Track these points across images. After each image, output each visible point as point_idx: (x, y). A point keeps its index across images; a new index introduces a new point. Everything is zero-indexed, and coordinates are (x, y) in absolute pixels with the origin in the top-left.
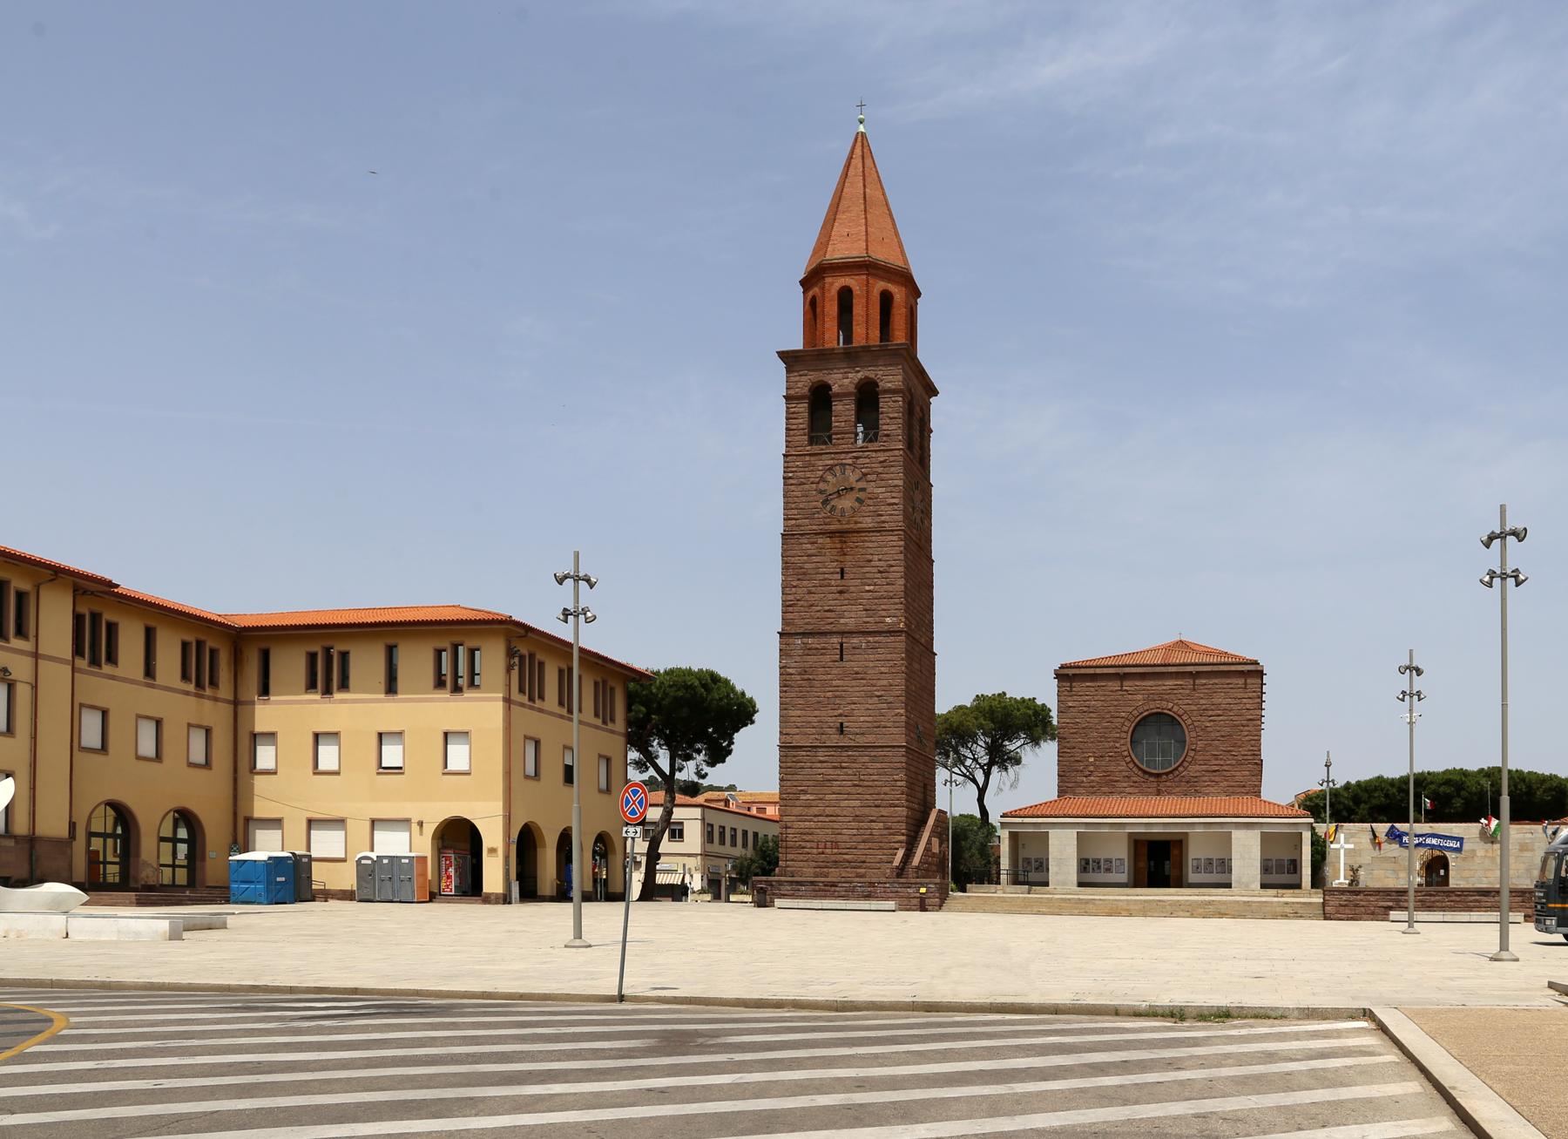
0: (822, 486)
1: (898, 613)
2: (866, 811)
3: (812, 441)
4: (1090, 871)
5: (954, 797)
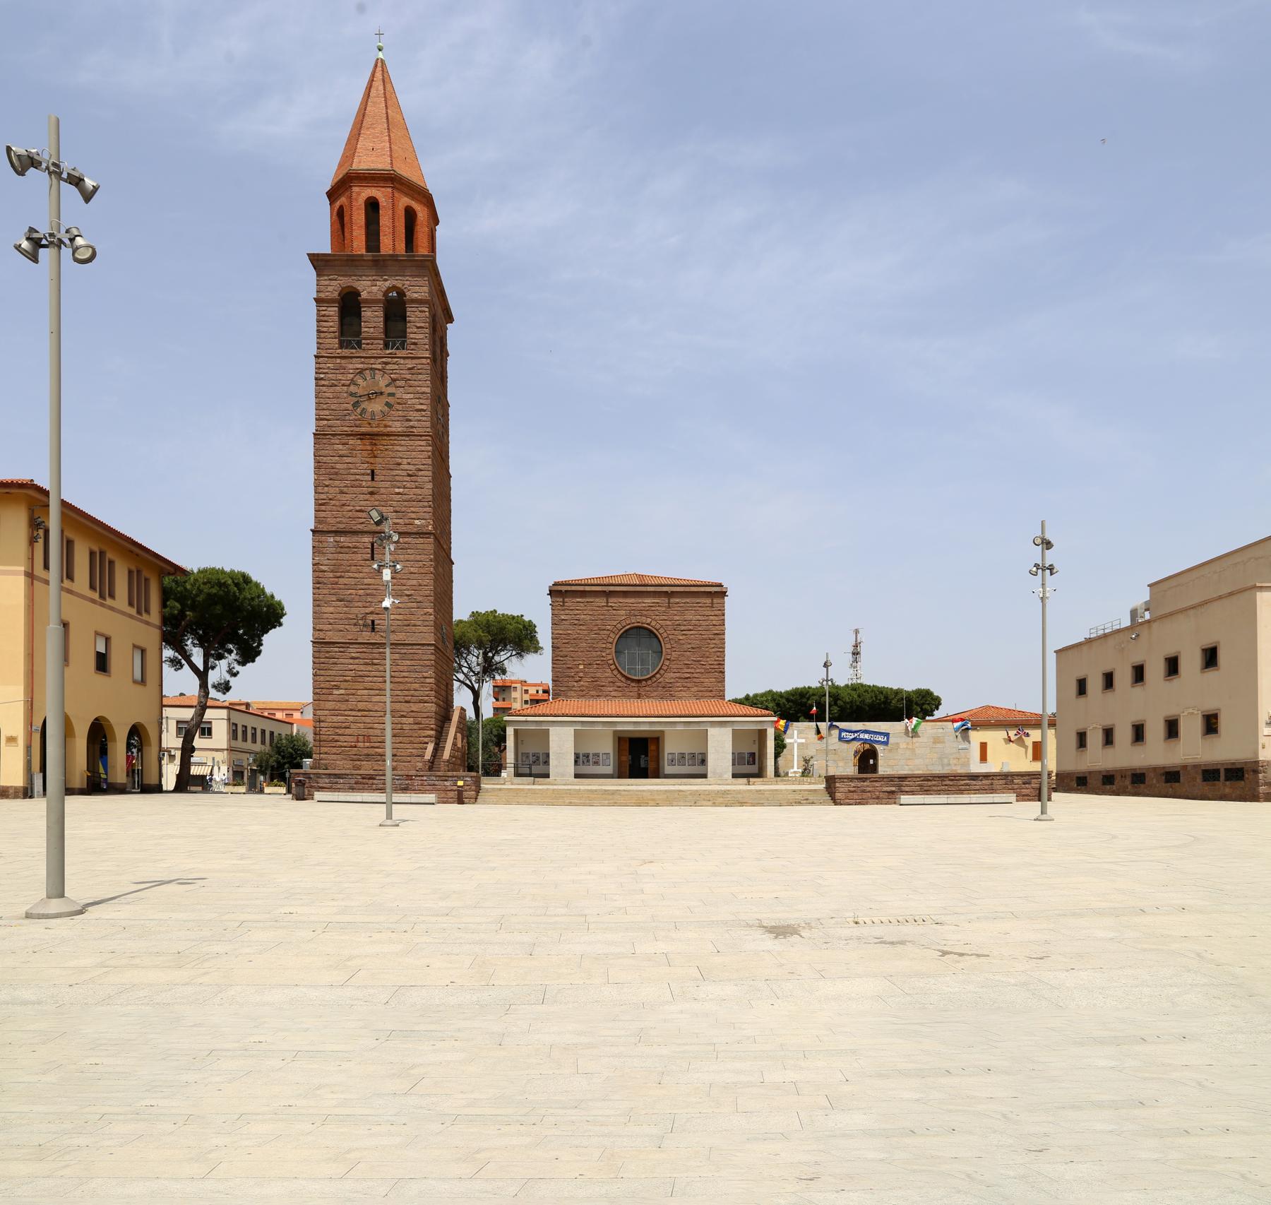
0: (353, 389)
1: (427, 516)
3: (342, 345)
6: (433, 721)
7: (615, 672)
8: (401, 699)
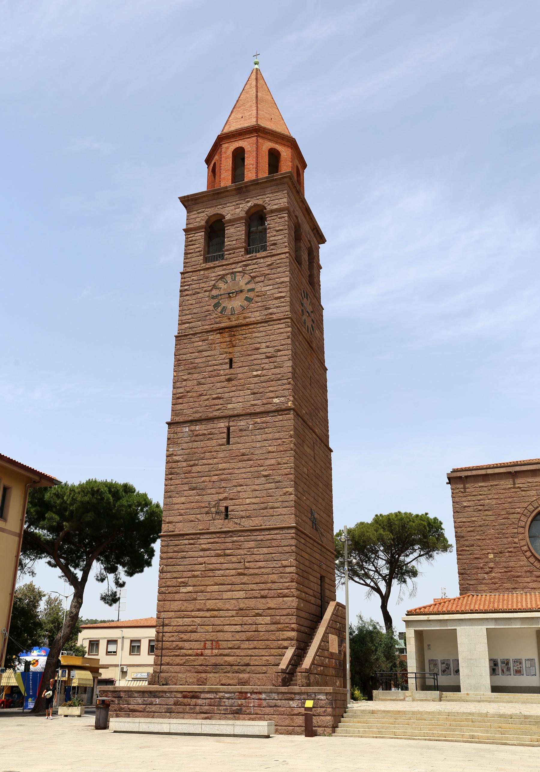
2: (251, 603)
3: (206, 260)
6: (294, 619)
8: (256, 594)
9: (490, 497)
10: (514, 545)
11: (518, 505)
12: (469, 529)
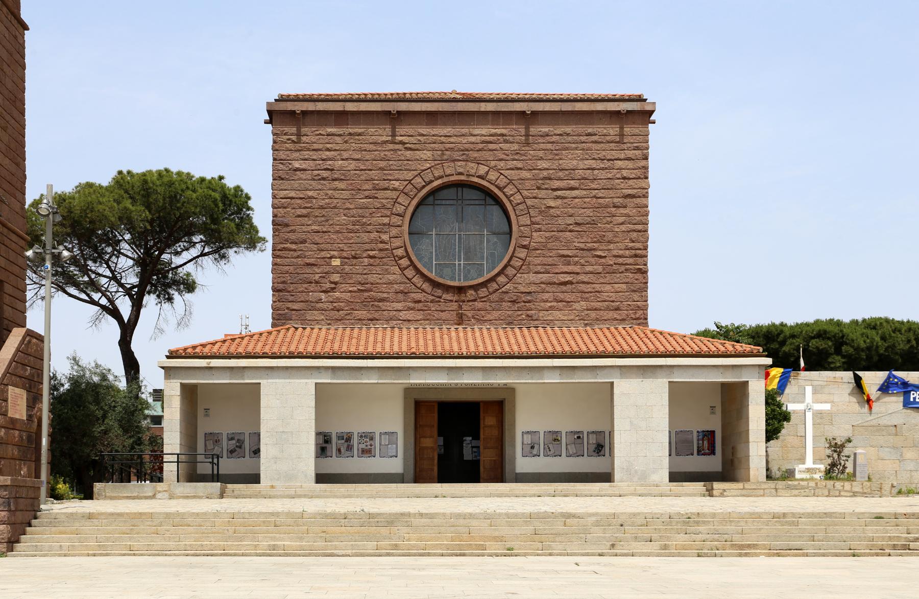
4: (337, 455)
5: (73, 334)
7: (410, 273)
9: (345, 155)
10: (381, 246)
11: (397, 175)
12: (299, 212)
